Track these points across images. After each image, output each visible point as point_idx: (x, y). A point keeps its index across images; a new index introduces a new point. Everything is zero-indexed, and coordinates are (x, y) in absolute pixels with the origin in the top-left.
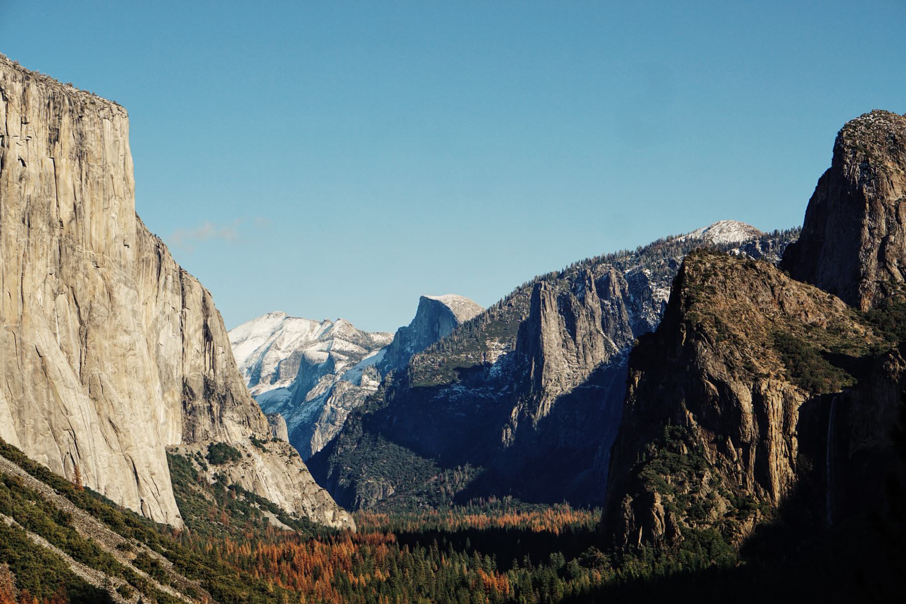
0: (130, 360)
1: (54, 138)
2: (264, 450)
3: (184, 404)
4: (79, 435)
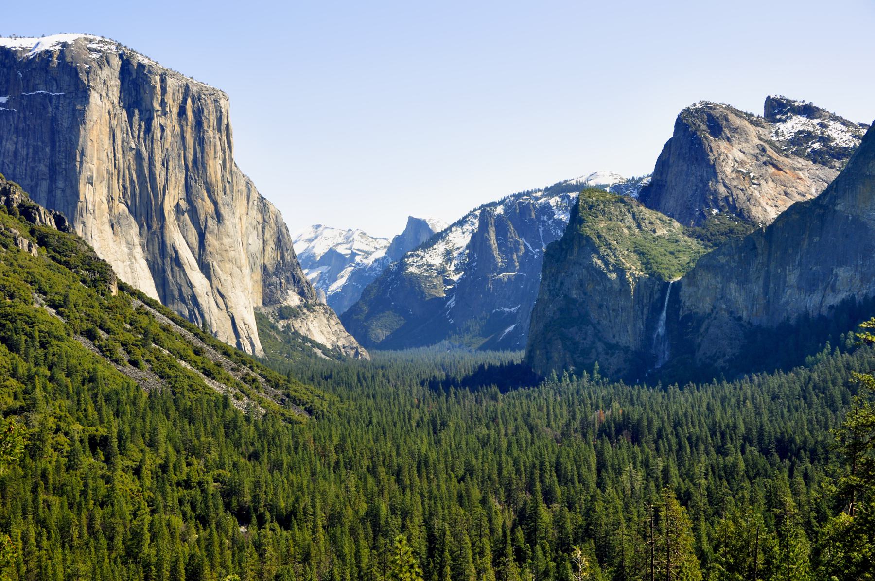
0: (232, 254)
1: (182, 112)
2: (314, 311)
3: (264, 281)
4: (200, 300)
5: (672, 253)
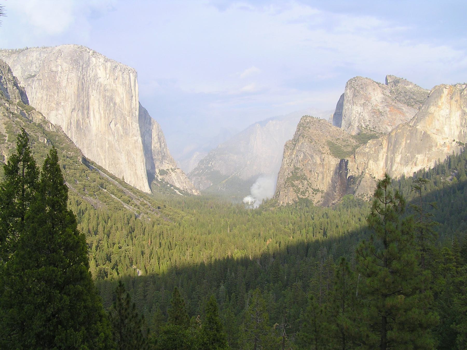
5: (344, 146)
